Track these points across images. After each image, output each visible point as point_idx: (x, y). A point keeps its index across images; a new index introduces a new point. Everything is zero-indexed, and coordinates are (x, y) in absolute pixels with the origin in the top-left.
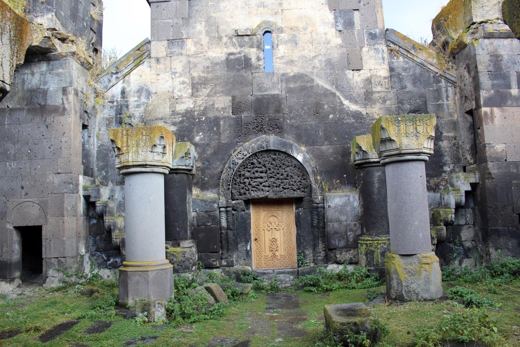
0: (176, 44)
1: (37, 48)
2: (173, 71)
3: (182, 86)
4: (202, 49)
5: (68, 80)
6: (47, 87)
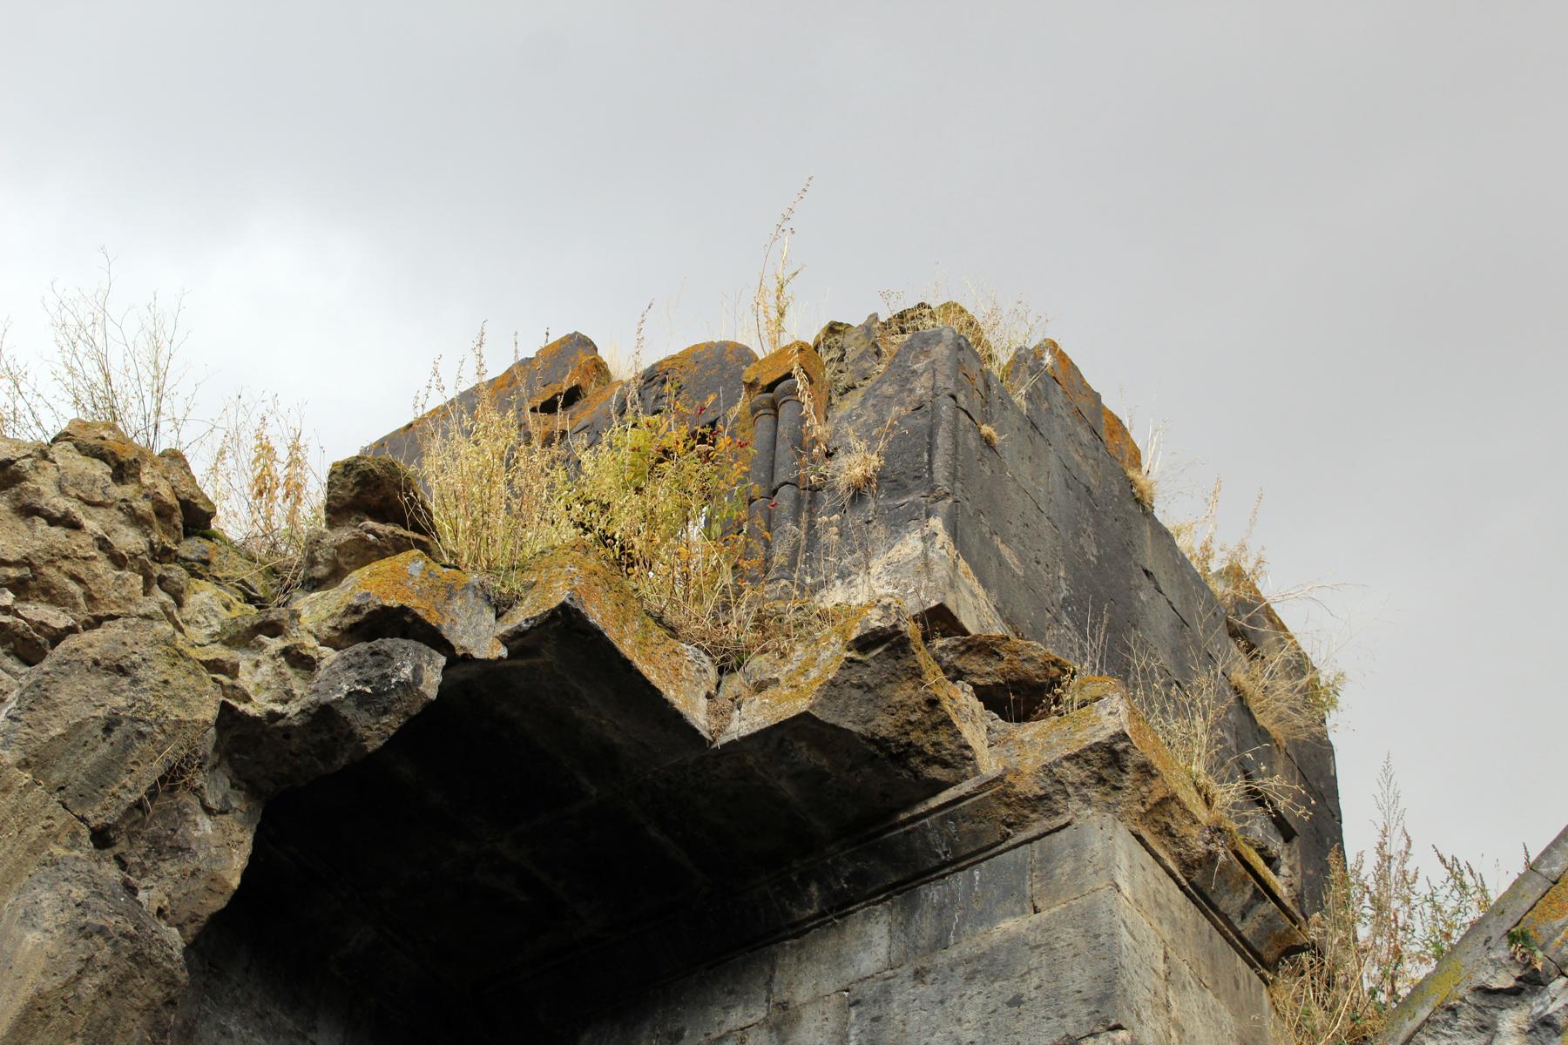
1: (806, 755)
5: (1079, 978)
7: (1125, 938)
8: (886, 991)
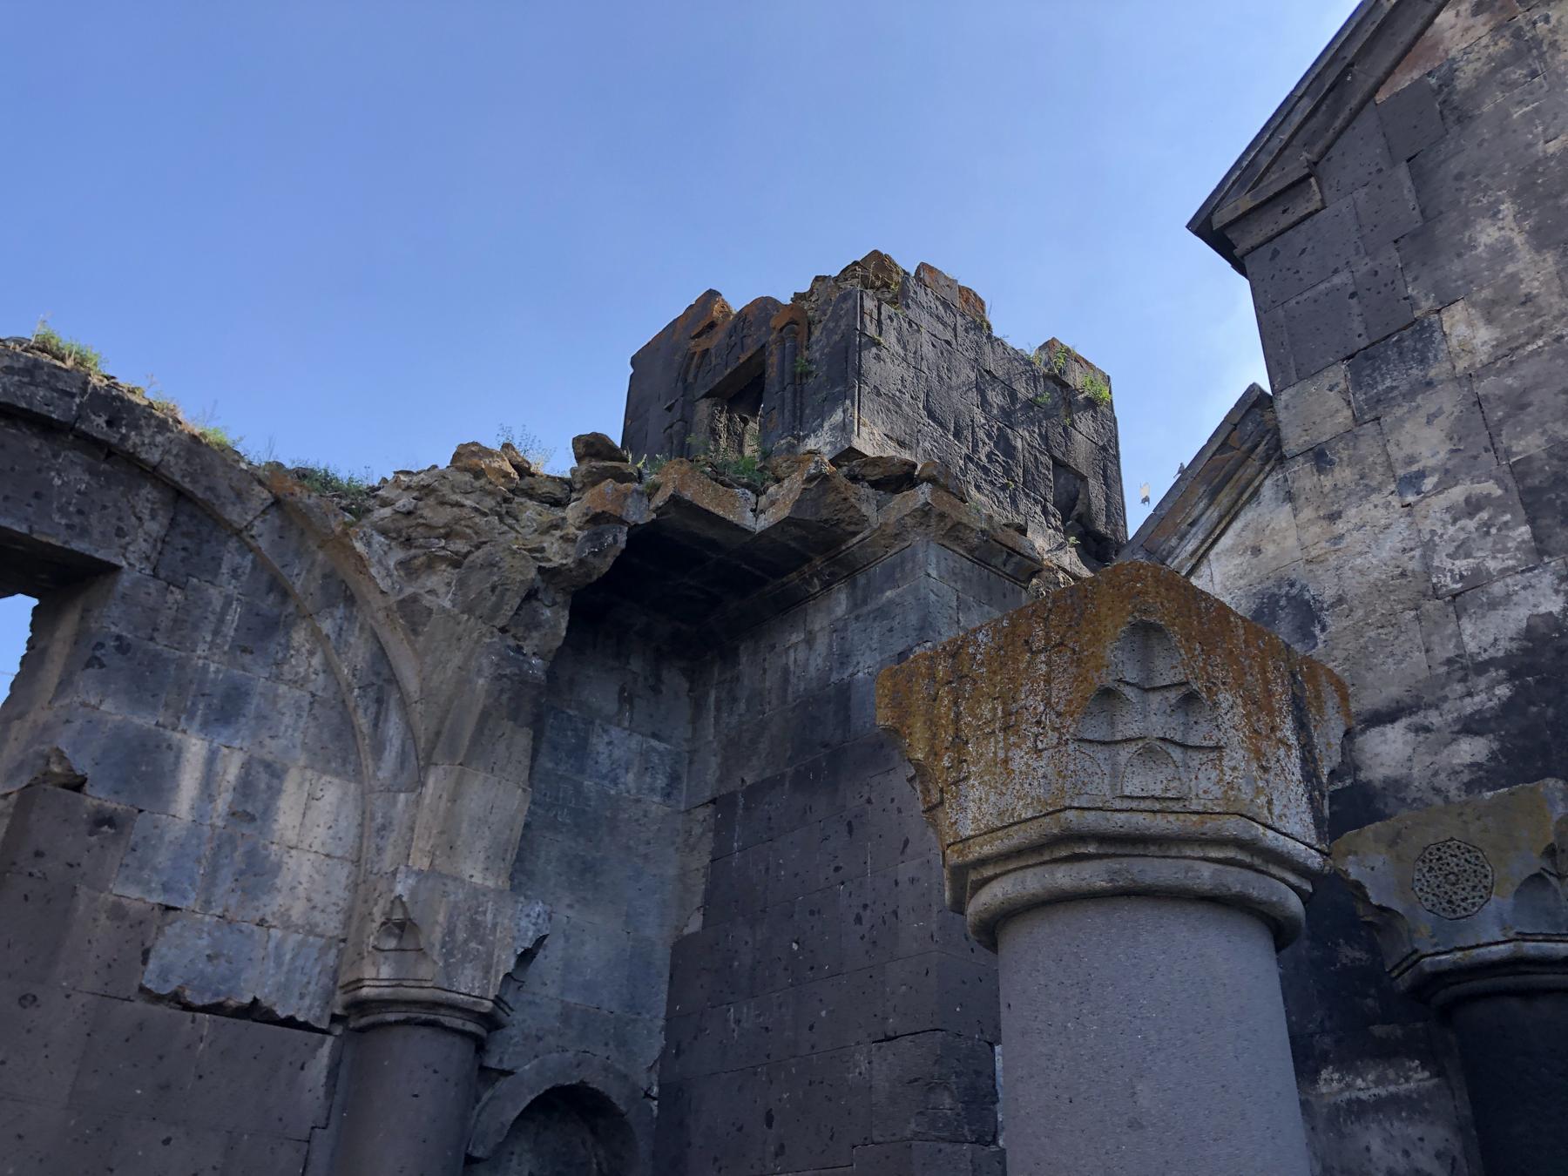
0: (1392, 354)
2: (1401, 472)
3: (1471, 524)
4: (1534, 316)
5: (913, 619)
6: (850, 670)
7: (932, 597)
8: (846, 625)
